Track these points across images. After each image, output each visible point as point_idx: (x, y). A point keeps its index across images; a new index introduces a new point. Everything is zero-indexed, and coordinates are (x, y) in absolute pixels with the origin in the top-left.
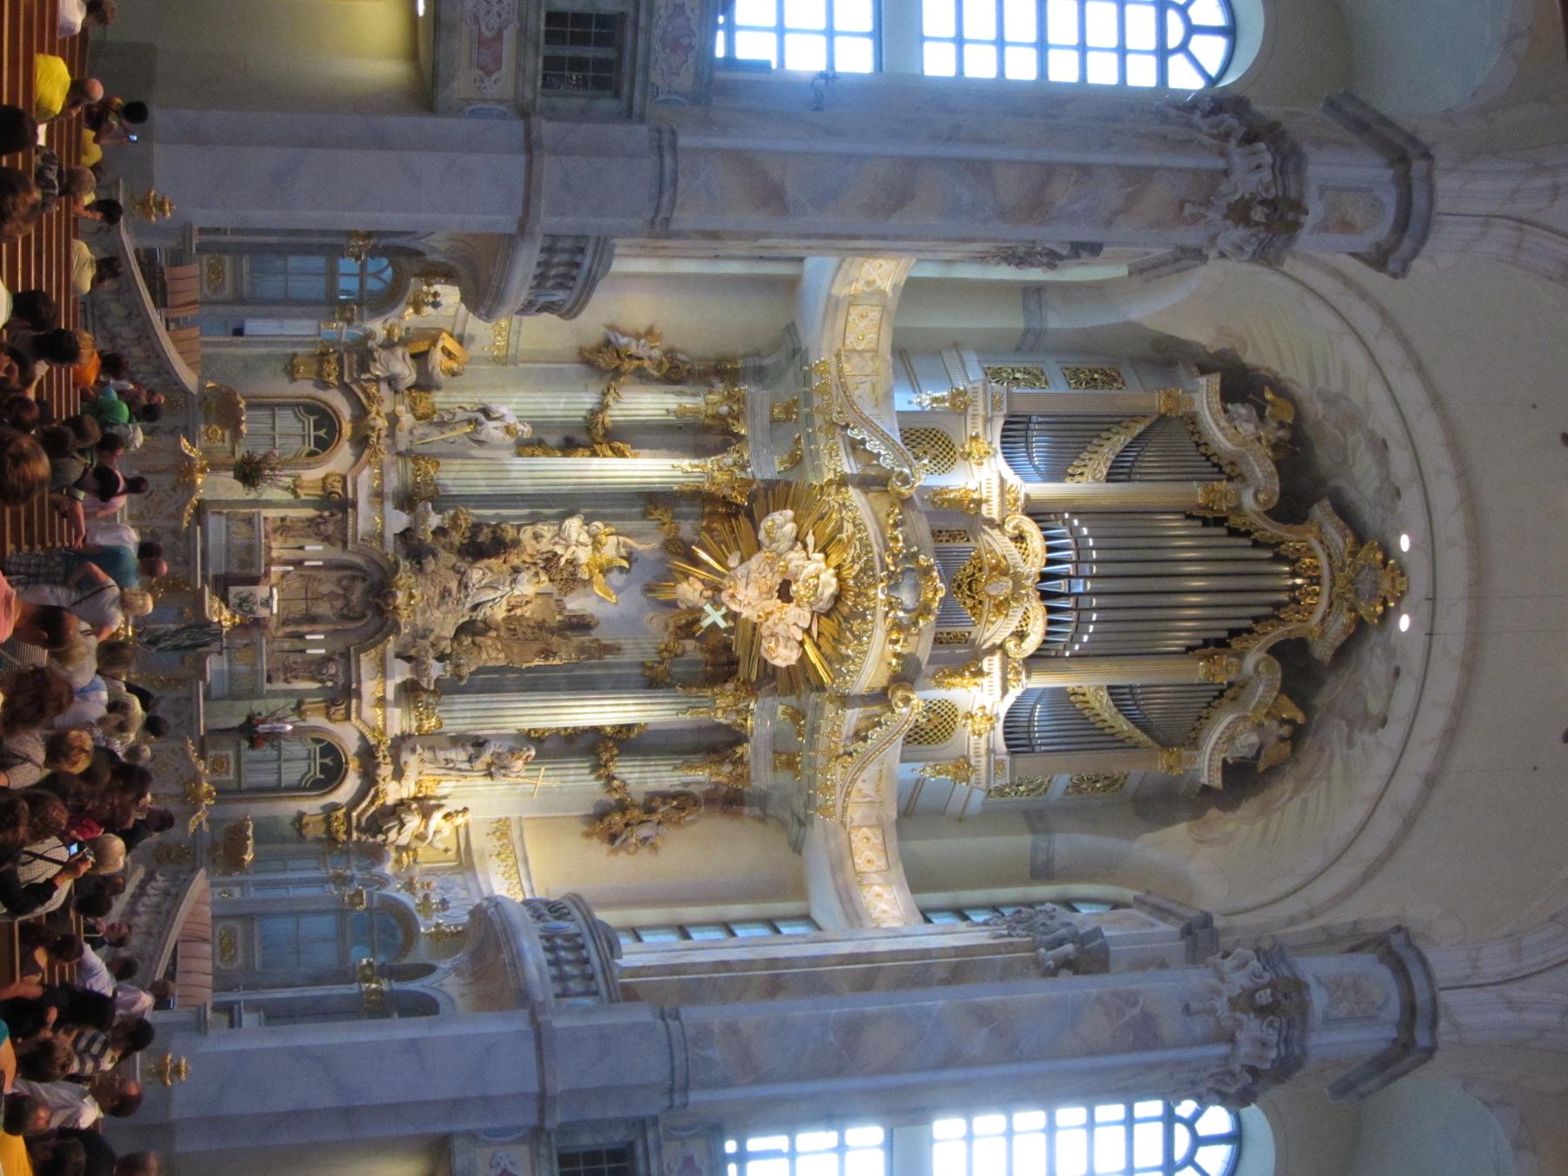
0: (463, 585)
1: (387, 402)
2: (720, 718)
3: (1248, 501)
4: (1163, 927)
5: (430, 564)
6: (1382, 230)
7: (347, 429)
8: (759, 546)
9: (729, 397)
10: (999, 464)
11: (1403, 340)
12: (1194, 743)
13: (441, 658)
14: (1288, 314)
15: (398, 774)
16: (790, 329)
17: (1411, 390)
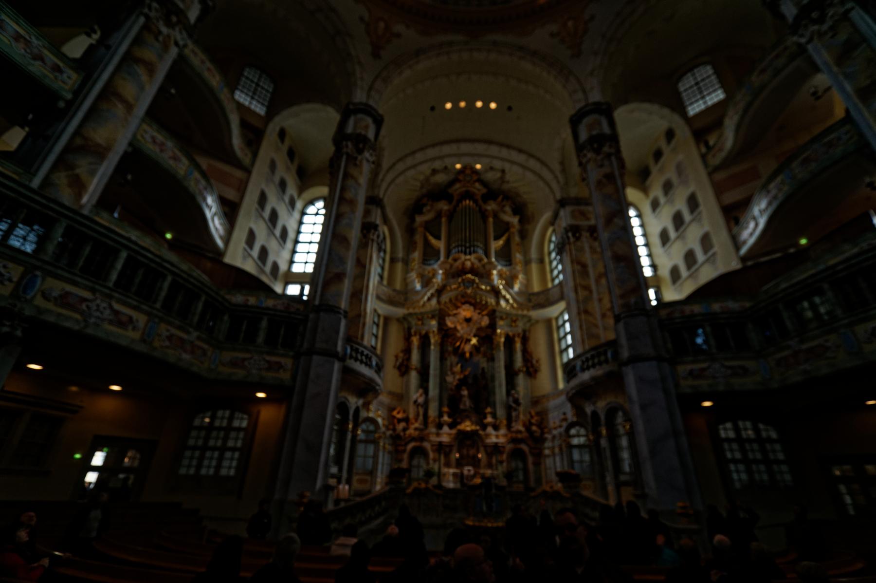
0: (465, 411)
1: (411, 431)
2: (503, 340)
3: (446, 208)
4: (562, 213)
5: (459, 420)
6: (369, 121)
7: (418, 444)
8: (455, 328)
9: (415, 335)
10: (436, 266)
11: (406, 156)
12: (508, 223)
13: (485, 418)
14: (398, 191)
15: (520, 432)
16: (398, 320)
17: (419, 157)
